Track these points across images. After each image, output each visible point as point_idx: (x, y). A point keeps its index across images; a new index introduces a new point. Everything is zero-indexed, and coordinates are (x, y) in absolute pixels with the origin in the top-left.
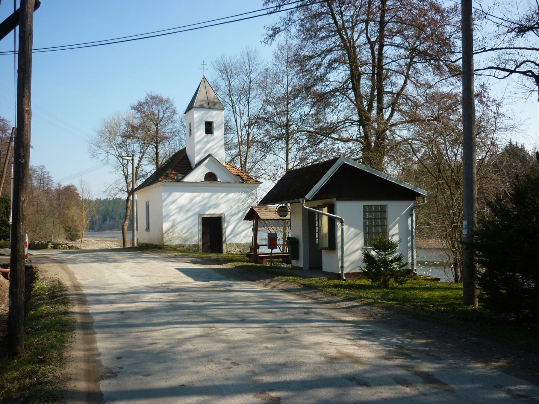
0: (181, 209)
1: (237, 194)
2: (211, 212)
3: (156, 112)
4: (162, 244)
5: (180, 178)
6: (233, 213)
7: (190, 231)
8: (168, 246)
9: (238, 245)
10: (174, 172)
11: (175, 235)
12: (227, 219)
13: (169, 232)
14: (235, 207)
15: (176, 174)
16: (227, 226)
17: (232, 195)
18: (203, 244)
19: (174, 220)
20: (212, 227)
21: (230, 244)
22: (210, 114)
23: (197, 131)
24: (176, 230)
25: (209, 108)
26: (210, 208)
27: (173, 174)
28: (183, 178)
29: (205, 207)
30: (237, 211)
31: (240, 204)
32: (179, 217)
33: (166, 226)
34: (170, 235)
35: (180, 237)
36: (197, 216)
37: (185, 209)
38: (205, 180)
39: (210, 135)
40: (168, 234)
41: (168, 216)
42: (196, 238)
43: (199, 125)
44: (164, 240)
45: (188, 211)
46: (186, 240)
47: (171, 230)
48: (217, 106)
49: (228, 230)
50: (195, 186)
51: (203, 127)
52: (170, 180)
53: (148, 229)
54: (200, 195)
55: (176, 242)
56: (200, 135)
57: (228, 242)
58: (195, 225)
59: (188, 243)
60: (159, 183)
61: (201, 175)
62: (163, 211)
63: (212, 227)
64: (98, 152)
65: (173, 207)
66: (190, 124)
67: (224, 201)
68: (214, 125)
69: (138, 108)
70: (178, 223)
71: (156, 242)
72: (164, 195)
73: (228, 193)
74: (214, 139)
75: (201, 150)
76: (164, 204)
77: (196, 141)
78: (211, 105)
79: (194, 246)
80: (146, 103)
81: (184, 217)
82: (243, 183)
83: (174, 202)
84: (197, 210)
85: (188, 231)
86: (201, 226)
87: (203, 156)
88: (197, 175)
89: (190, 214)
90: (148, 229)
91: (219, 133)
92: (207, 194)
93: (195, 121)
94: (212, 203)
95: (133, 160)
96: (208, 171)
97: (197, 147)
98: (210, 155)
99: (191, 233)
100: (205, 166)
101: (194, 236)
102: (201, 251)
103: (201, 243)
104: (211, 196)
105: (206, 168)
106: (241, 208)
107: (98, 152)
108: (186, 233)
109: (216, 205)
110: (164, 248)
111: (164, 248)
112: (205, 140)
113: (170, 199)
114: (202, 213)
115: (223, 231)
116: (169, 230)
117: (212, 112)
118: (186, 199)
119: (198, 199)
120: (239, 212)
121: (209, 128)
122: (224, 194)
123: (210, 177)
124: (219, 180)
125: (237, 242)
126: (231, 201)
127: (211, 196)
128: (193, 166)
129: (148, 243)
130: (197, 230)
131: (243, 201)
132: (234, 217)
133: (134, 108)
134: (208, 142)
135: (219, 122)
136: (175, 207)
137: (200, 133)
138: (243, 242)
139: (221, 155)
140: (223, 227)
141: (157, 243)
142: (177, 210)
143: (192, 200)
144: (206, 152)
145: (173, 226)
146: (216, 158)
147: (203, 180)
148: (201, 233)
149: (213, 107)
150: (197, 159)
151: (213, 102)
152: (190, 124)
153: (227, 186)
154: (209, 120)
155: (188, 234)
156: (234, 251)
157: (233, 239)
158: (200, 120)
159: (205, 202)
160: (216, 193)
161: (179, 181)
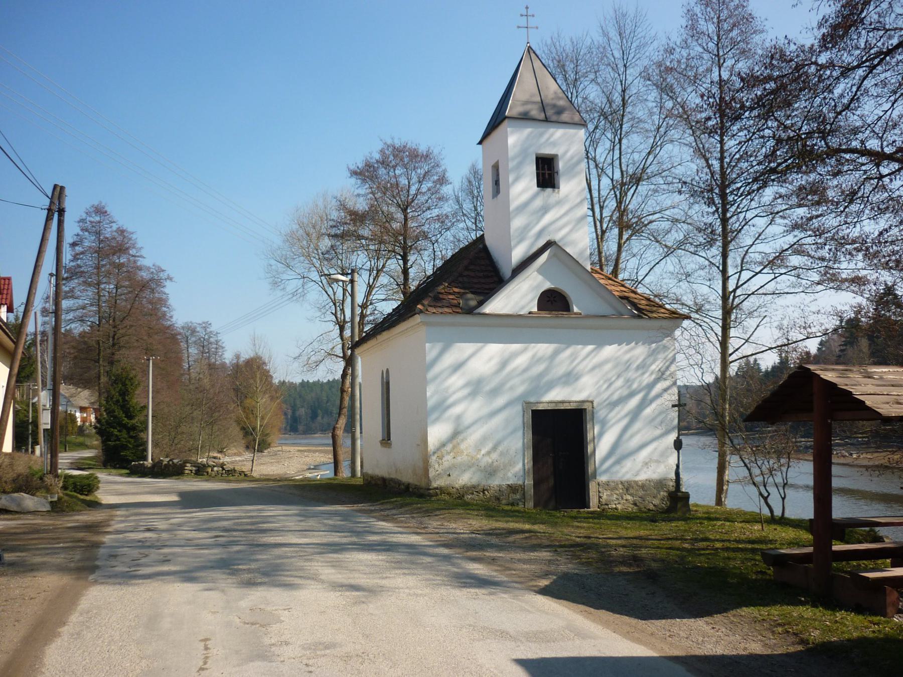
0: (476, 387)
1: (625, 347)
2: (556, 396)
3: (403, 181)
4: (423, 484)
5: (473, 303)
6: (616, 397)
7: (500, 448)
8: (442, 490)
9: (628, 486)
10: (456, 290)
11: (459, 459)
12: (601, 414)
13: (444, 450)
14: (620, 382)
15: (461, 295)
16: (601, 434)
17: (609, 350)
18: (537, 484)
19: (459, 418)
20: (559, 436)
21: (607, 484)
22: (546, 136)
23: (517, 179)
24: (463, 446)
25: (546, 120)
26: (550, 386)
27: (454, 293)
28: (481, 303)
29: (540, 384)
30: (625, 392)
31: (631, 374)
32: (472, 409)
33: (436, 433)
34: (448, 460)
35: (473, 464)
36: (518, 408)
37: (487, 388)
38: (539, 309)
39: (549, 190)
40: (441, 458)
41: (442, 407)
42: (519, 466)
43: (520, 165)
44: (432, 473)
45: (495, 392)
46: (491, 471)
47: (449, 447)
48: (565, 117)
49: (602, 444)
50: (511, 326)
51: (530, 170)
52: (446, 310)
53: (386, 439)
54: (525, 349)
55: (465, 479)
56: (524, 191)
57: (603, 478)
58: (514, 431)
59: (496, 482)
60: (418, 318)
61: (530, 297)
62: (428, 394)
63: (559, 436)
64: (285, 277)
65: (456, 381)
66: (496, 168)
67: (590, 367)
68: (561, 165)
69: (365, 173)
70: (468, 427)
71: (407, 477)
72: (431, 350)
73: (601, 344)
74: (559, 203)
75: (526, 228)
76: (430, 375)
77: (513, 206)
78: (550, 112)
79: (513, 489)
80: (384, 163)
81: (486, 410)
82: (639, 317)
83: (457, 367)
84: (521, 390)
85: (494, 448)
87: (532, 245)
88: (518, 297)
89: (500, 401)
90: (386, 439)
91: (571, 186)
92: (544, 349)
93: (511, 153)
94: (561, 369)
95: (352, 281)
96: (548, 285)
97: (517, 223)
99: (502, 454)
100: (540, 271)
101: (512, 464)
102: (530, 504)
103: (529, 482)
104: (556, 353)
105: (540, 278)
106: (635, 386)
107: (285, 277)
108: (489, 453)
109: (570, 378)
110: (431, 496)
111: (431, 496)
112: (538, 203)
113: (449, 359)
114: (532, 400)
115: (590, 448)
116: (443, 445)
117: (552, 130)
118: (490, 359)
119: (521, 361)
120: (632, 395)
121: (547, 172)
122: (590, 347)
123: (553, 301)
124: (576, 309)
125: (625, 479)
126: (608, 367)
127: (556, 353)
128: (506, 272)
129: (386, 475)
131: (638, 368)
132: (617, 409)
133: (354, 173)
134: (545, 209)
135: (572, 158)
136: (461, 382)
137: (523, 186)
138: (642, 477)
139: (580, 242)
140: (589, 436)
141: (411, 481)
142: (466, 391)
143: (504, 364)
145: (456, 434)
146: (568, 250)
147: (535, 309)
148: (529, 454)
149: (554, 118)
150: (518, 254)
151: (554, 106)
152: (496, 168)
153: (599, 328)
154: (547, 151)
155: (494, 456)
156: (621, 503)
157: (617, 468)
158: (524, 152)
159: (541, 367)
160: (569, 344)
161: (470, 311)
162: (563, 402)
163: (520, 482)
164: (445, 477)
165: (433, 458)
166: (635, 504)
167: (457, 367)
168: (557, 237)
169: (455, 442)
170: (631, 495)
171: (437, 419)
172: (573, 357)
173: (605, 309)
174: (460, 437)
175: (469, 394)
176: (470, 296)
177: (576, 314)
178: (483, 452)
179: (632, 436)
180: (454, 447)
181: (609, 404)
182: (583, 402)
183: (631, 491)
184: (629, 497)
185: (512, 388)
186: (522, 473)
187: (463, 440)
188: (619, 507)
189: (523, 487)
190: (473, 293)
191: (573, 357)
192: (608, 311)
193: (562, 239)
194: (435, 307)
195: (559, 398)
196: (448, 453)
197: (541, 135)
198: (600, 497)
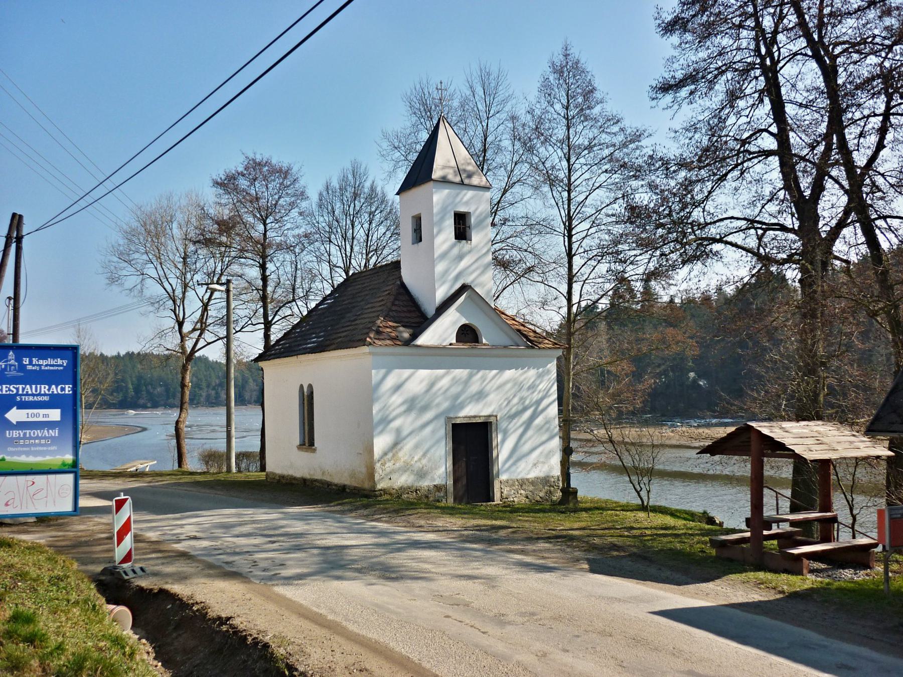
0: (412, 405)
1: (520, 371)
2: (470, 411)
4: (367, 485)
5: (406, 335)
6: (514, 410)
8: (385, 491)
9: (522, 483)
10: (391, 324)
11: (398, 465)
12: (503, 425)
14: (516, 400)
16: (503, 441)
17: (509, 374)
19: (398, 431)
20: (472, 443)
21: (507, 481)
23: (439, 232)
25: (462, 183)
27: (390, 327)
28: (415, 336)
30: (520, 408)
31: (524, 393)
32: (406, 423)
36: (442, 421)
38: (457, 341)
39: (464, 241)
41: (386, 421)
45: (425, 409)
47: (390, 455)
49: (503, 449)
50: (437, 356)
51: (450, 223)
55: (403, 480)
56: (444, 242)
57: (504, 477)
58: (438, 441)
59: (426, 484)
60: (365, 349)
61: (450, 331)
62: (374, 412)
63: (472, 443)
64: (124, 273)
66: (417, 220)
67: (495, 387)
69: (227, 184)
73: (502, 368)
75: (446, 272)
79: (438, 488)
85: (424, 455)
86: (450, 445)
88: (441, 332)
89: (429, 415)
91: (480, 237)
92: (461, 373)
96: (464, 321)
97: (440, 268)
98: (464, 288)
99: (430, 460)
101: (437, 468)
102: (451, 500)
103: (450, 482)
104: (471, 376)
105: (458, 314)
106: (527, 402)
107: (124, 273)
108: (420, 460)
109: (480, 396)
111: (376, 496)
112: (455, 251)
113: (390, 382)
114: (452, 415)
115: (495, 454)
116: (385, 454)
118: (421, 382)
119: (445, 382)
120: (525, 409)
121: (462, 227)
122: (494, 372)
123: (467, 334)
124: (484, 341)
125: (519, 477)
126: (509, 386)
127: (471, 376)
130: (443, 452)
131: (529, 388)
132: (514, 421)
133: (217, 184)
134: (461, 257)
135: (481, 214)
136: (400, 400)
138: (532, 475)
140: (494, 444)
141: (347, 483)
142: (403, 408)
143: (432, 385)
144: (457, 278)
145: (396, 444)
147: (454, 341)
150: (441, 294)
152: (417, 220)
153: (501, 356)
154: (462, 209)
155: (424, 461)
156: (518, 498)
158: (444, 210)
160: (479, 368)
161: (408, 343)
162: (475, 417)
163: (444, 483)
164: (387, 480)
165: (378, 466)
166: (527, 497)
167: (398, 388)
168: (468, 280)
169: (394, 451)
170: (524, 490)
171: (381, 432)
172: (483, 379)
173: (505, 341)
174: (399, 447)
175: (405, 412)
176: (401, 329)
177: (485, 345)
178: (416, 459)
179: (524, 444)
180: (394, 456)
181: (509, 417)
182: (490, 416)
183: (524, 487)
184: (523, 492)
185: (438, 405)
186: (444, 475)
187: (400, 450)
188: (516, 499)
189: (445, 486)
190: (404, 326)
191: (483, 379)
192: (507, 342)
193: (473, 282)
194: (379, 339)
195: (472, 414)
196: (389, 461)
197: (458, 195)
198: (502, 493)
